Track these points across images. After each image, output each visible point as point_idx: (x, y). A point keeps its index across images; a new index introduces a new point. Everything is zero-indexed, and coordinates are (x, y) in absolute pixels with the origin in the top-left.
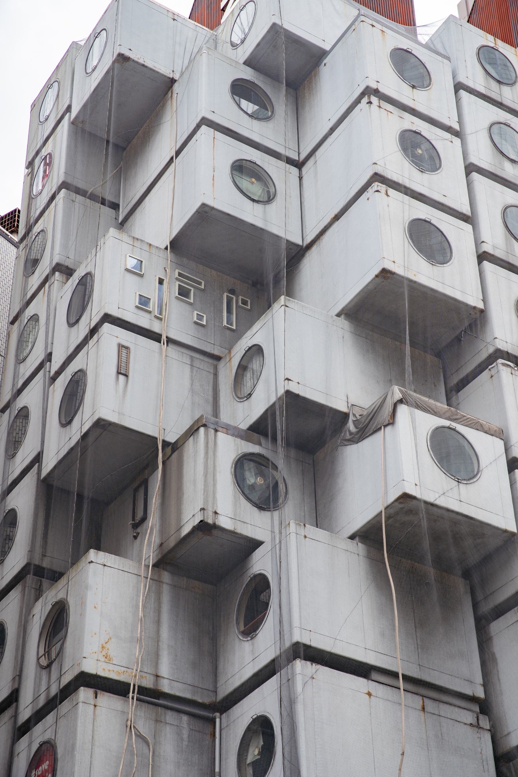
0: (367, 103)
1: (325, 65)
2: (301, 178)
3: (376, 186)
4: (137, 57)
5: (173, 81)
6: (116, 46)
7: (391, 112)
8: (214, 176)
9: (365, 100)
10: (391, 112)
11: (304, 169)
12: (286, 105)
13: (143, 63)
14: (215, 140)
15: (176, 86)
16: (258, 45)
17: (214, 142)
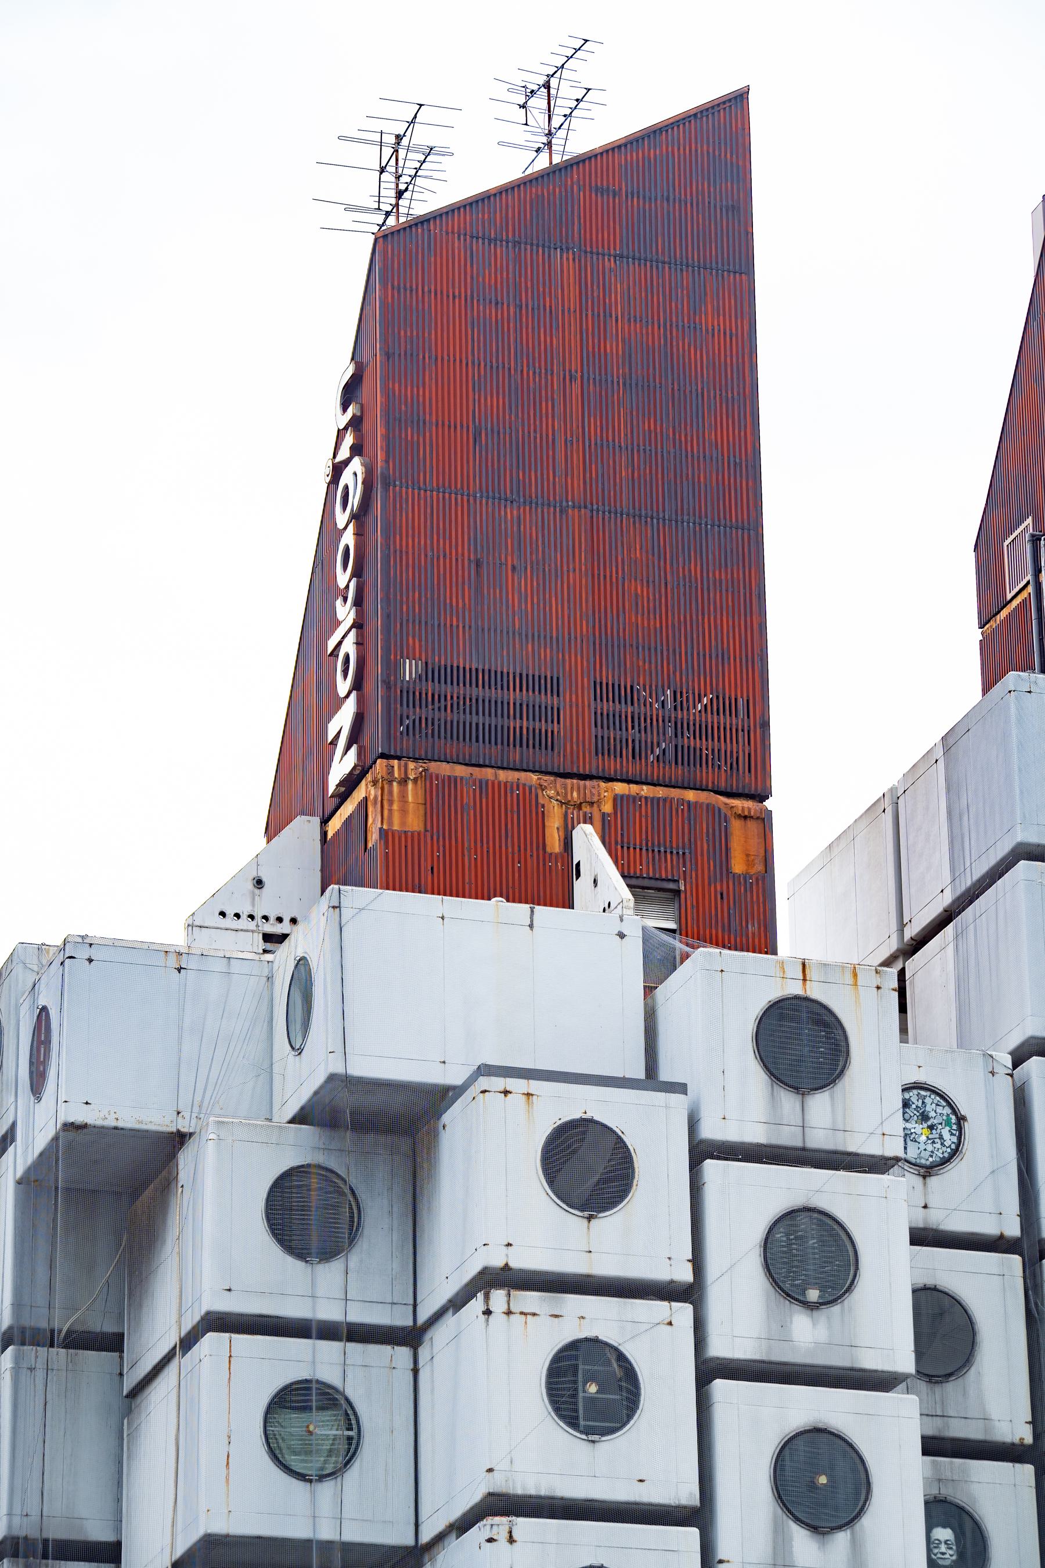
0: (484, 1313)
1: (444, 1127)
2: (416, 1371)
3: (488, 1527)
4: (102, 1115)
5: (181, 1139)
6: (62, 1107)
7: (534, 1314)
8: (228, 1456)
9: (477, 1304)
10: (534, 1314)
11: (424, 1353)
12: (390, 1189)
13: (114, 1124)
14: (232, 1359)
15: (185, 1159)
16: (316, 1093)
17: (230, 1369)
